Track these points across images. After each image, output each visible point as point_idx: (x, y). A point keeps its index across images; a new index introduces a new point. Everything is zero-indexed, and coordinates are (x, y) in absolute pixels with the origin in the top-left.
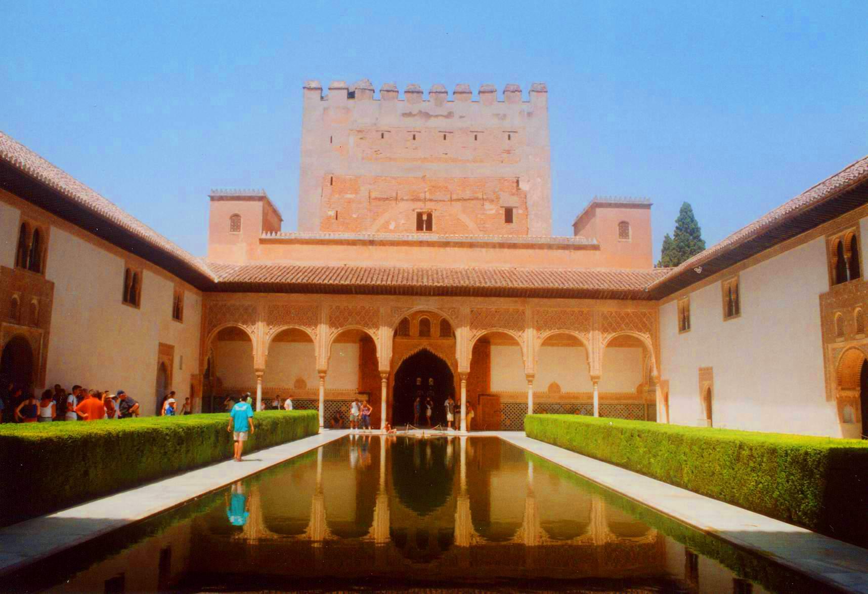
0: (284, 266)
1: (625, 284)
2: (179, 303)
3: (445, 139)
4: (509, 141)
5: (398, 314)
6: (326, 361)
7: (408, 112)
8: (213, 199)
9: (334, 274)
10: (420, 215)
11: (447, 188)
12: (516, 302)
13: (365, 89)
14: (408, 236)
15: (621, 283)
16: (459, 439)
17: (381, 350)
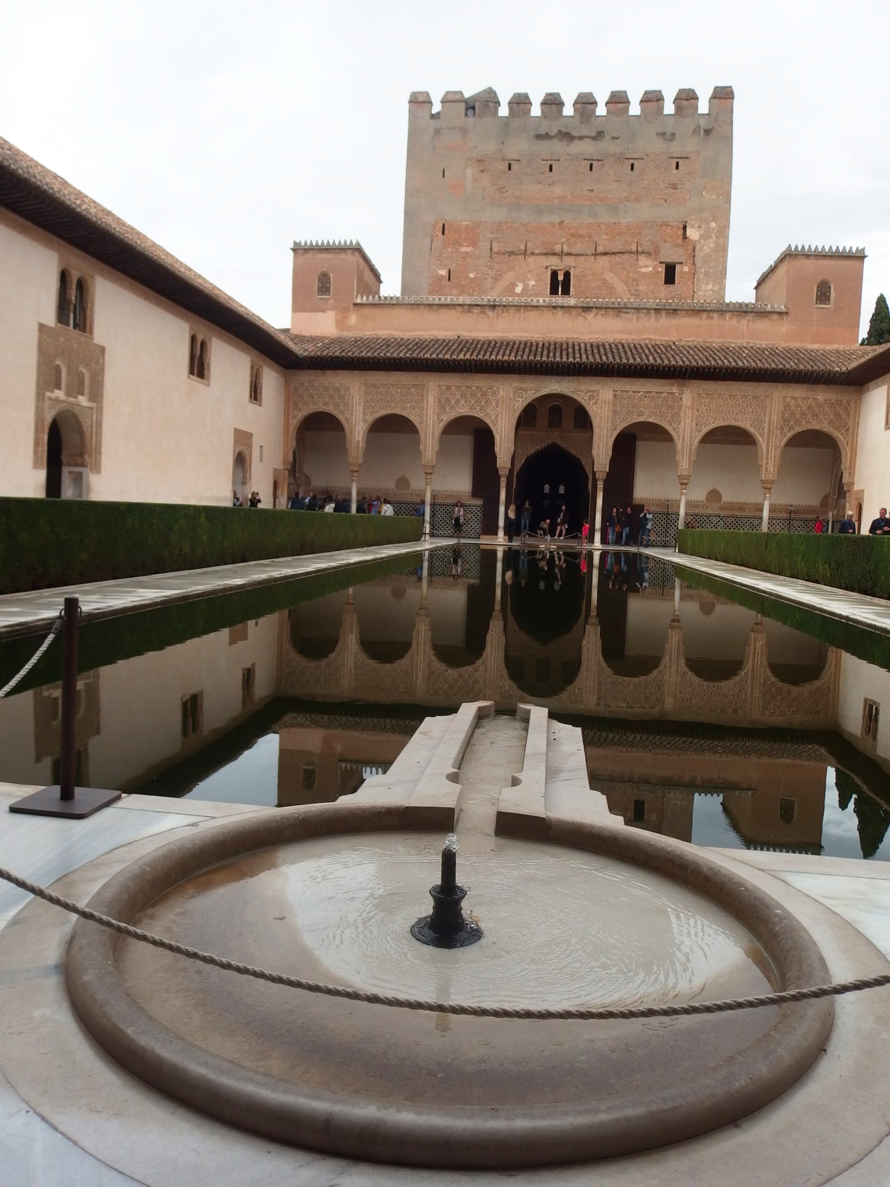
0: (383, 337)
1: (818, 363)
2: (257, 381)
3: (591, 169)
4: (675, 171)
5: (522, 397)
6: (434, 455)
7: (543, 133)
8: (294, 250)
9: (445, 347)
10: (554, 274)
11: (591, 238)
12: (673, 385)
13: (488, 101)
14: (538, 301)
15: (813, 362)
16: (593, 554)
17: (501, 442)
